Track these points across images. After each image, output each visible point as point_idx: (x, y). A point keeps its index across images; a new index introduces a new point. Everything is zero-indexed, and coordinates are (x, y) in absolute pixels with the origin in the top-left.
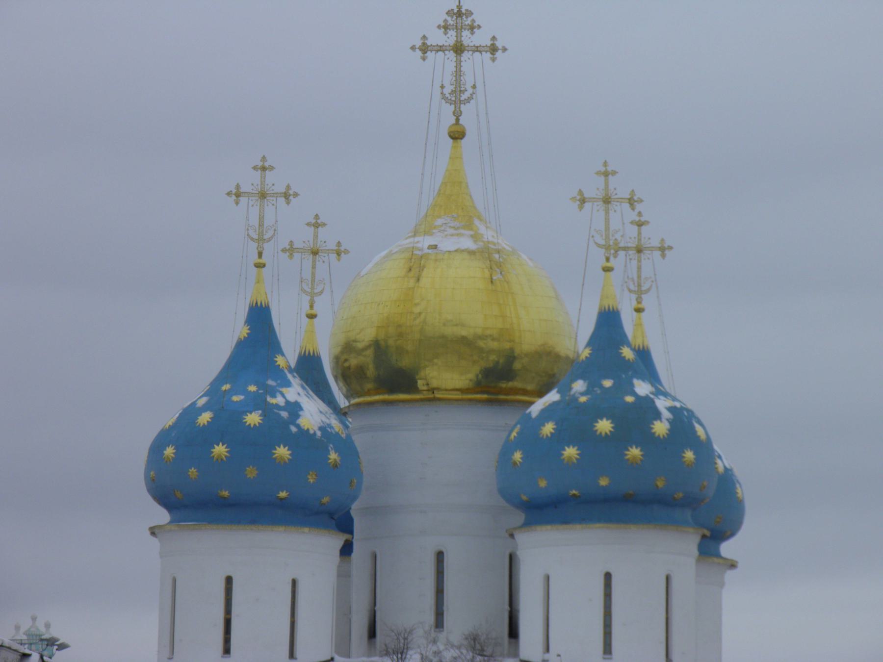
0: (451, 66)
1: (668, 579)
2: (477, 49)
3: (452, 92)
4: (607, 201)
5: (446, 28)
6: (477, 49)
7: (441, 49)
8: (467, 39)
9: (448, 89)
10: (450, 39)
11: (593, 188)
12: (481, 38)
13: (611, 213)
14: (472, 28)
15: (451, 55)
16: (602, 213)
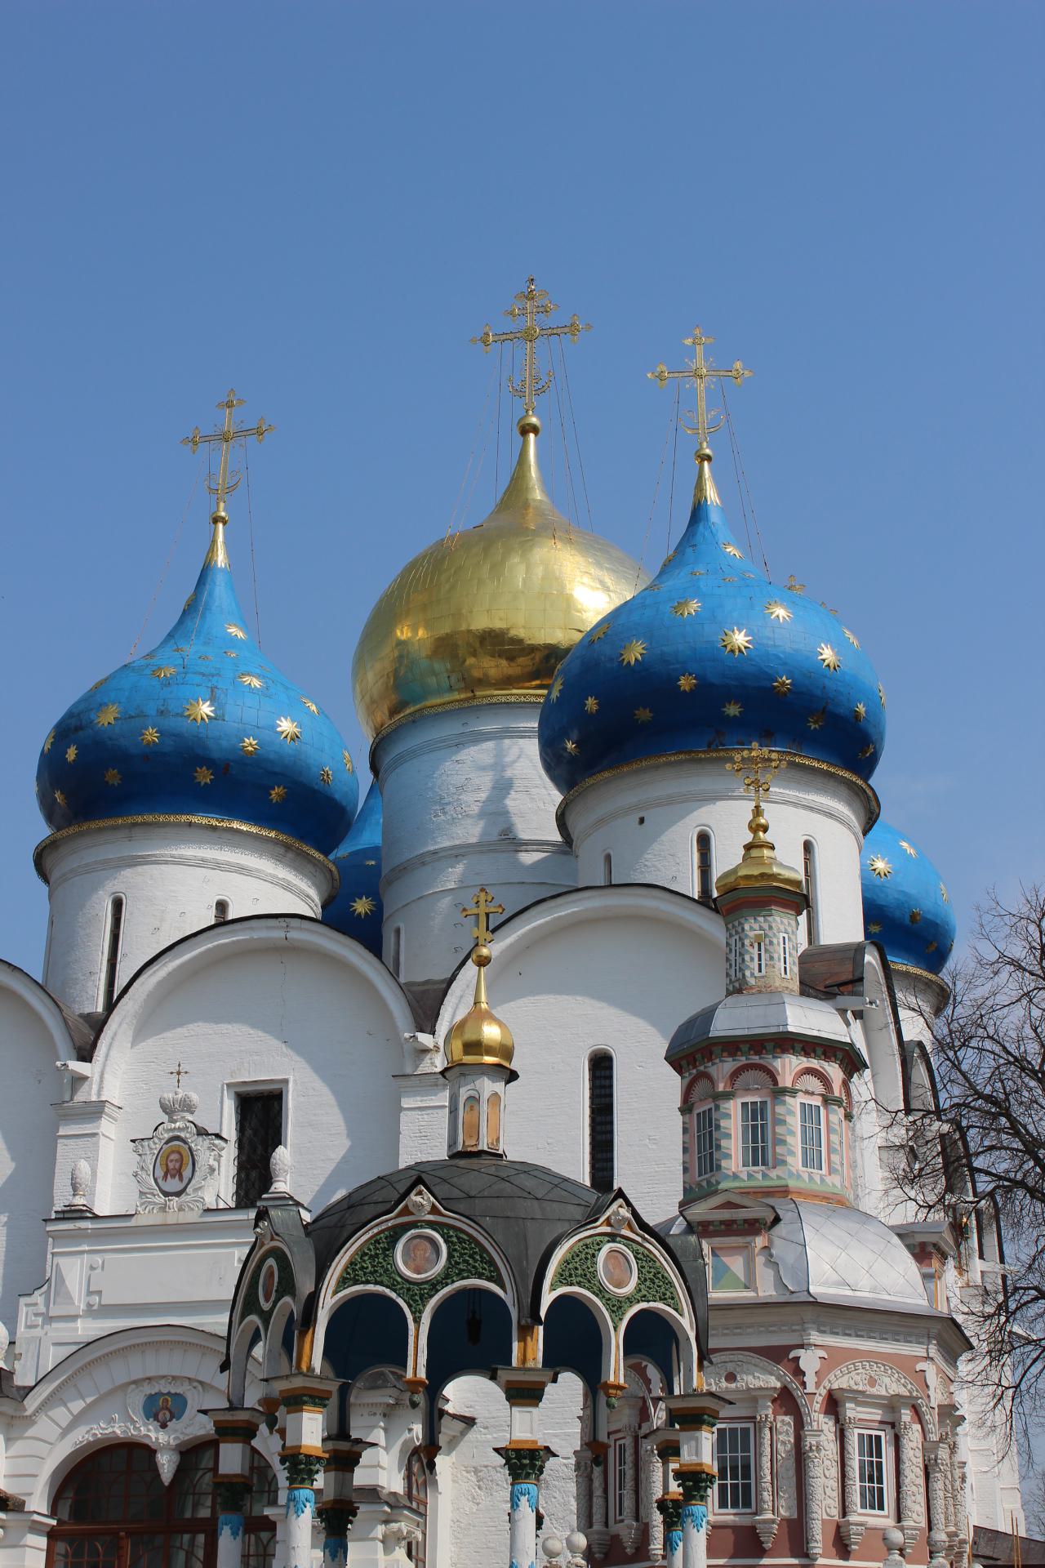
1: (808, 847)
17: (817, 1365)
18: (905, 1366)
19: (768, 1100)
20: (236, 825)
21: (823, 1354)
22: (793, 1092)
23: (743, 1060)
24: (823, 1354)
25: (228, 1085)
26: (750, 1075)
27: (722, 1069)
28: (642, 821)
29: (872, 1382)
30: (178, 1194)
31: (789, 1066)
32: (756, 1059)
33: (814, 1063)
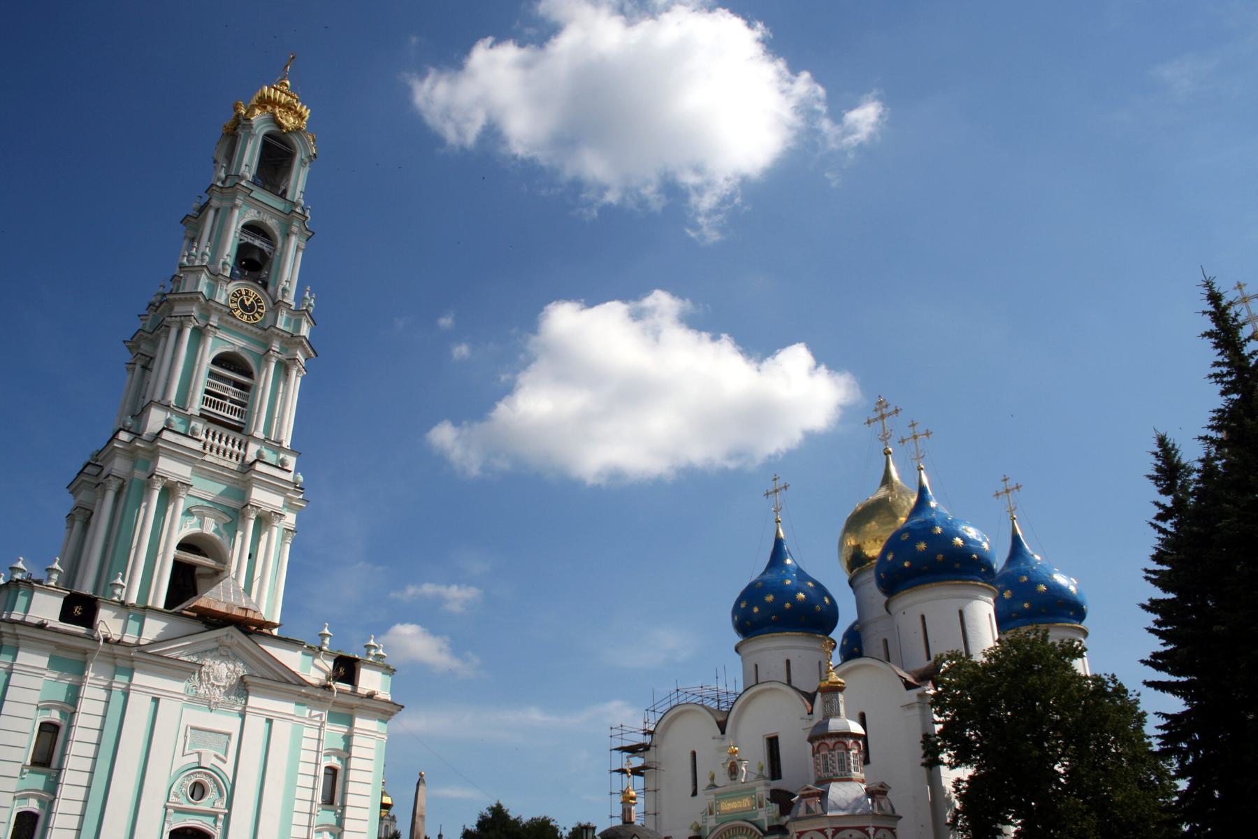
0: (881, 425)
2: (890, 414)
3: (883, 436)
4: (915, 437)
5: (876, 410)
6: (890, 414)
7: (876, 420)
8: (884, 412)
9: (882, 434)
10: (879, 414)
11: (907, 433)
12: (891, 409)
13: (918, 443)
14: (886, 406)
15: (880, 421)
16: (914, 444)
17: (832, 833)
18: (862, 829)
19: (828, 753)
20: (787, 633)
21: (834, 830)
22: (834, 749)
23: (820, 742)
24: (834, 830)
25: (764, 736)
26: (822, 746)
27: (816, 744)
28: (904, 613)
29: (851, 836)
30: (735, 779)
31: (831, 742)
32: (823, 741)
33: (841, 739)
